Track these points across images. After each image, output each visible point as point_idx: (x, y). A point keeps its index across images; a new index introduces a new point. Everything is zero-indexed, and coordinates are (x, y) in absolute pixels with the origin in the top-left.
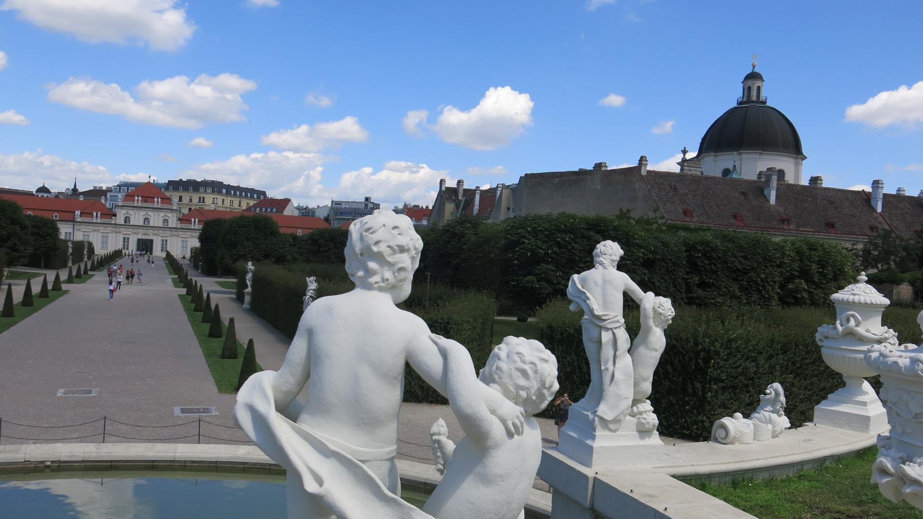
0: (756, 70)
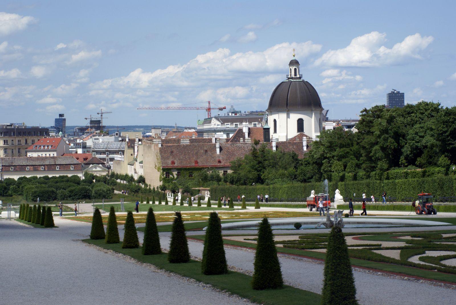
0: (296, 58)
